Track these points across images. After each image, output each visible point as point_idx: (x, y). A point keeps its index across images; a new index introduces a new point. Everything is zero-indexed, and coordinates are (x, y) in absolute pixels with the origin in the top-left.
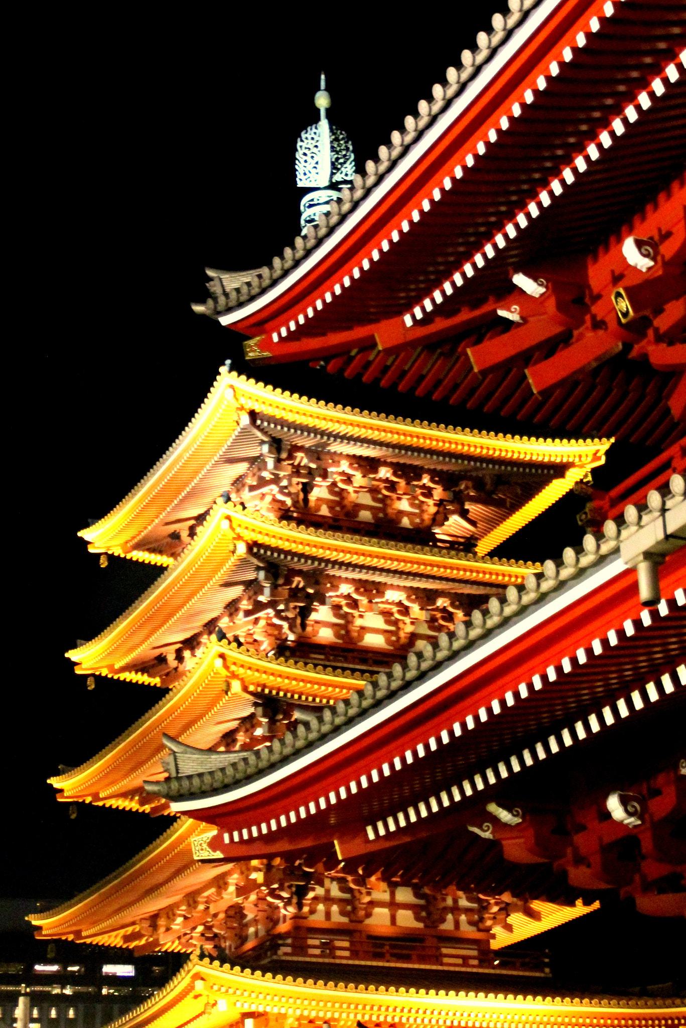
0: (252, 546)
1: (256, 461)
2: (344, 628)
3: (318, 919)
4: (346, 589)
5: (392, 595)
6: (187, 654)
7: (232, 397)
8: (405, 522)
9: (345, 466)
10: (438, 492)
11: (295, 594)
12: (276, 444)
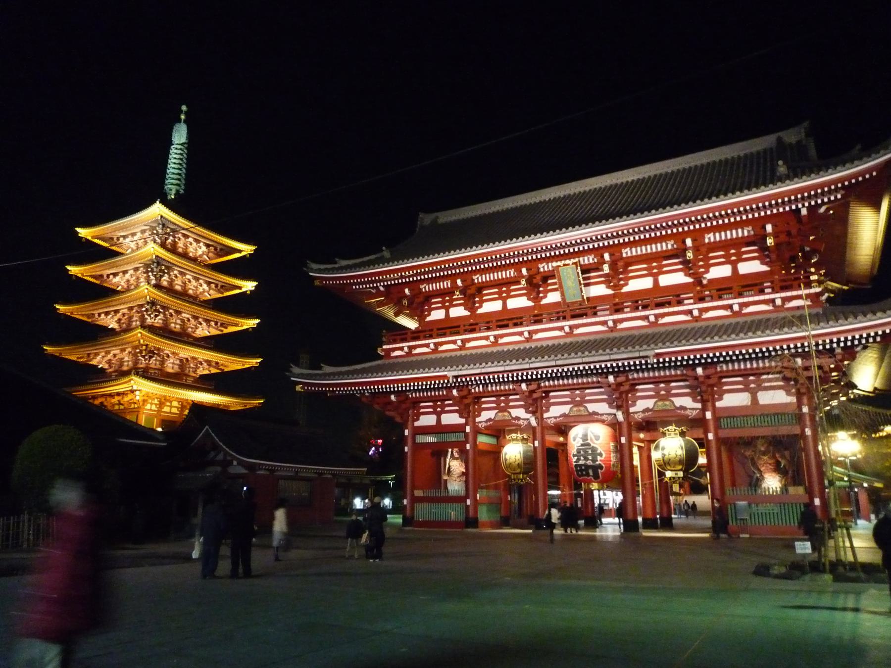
0: (157, 256)
1: (153, 228)
2: (171, 282)
3: (153, 366)
4: (176, 272)
5: (188, 277)
6: (111, 277)
7: (158, 210)
8: (191, 255)
9: (180, 235)
10: (204, 248)
11: (161, 271)
12: (163, 225)
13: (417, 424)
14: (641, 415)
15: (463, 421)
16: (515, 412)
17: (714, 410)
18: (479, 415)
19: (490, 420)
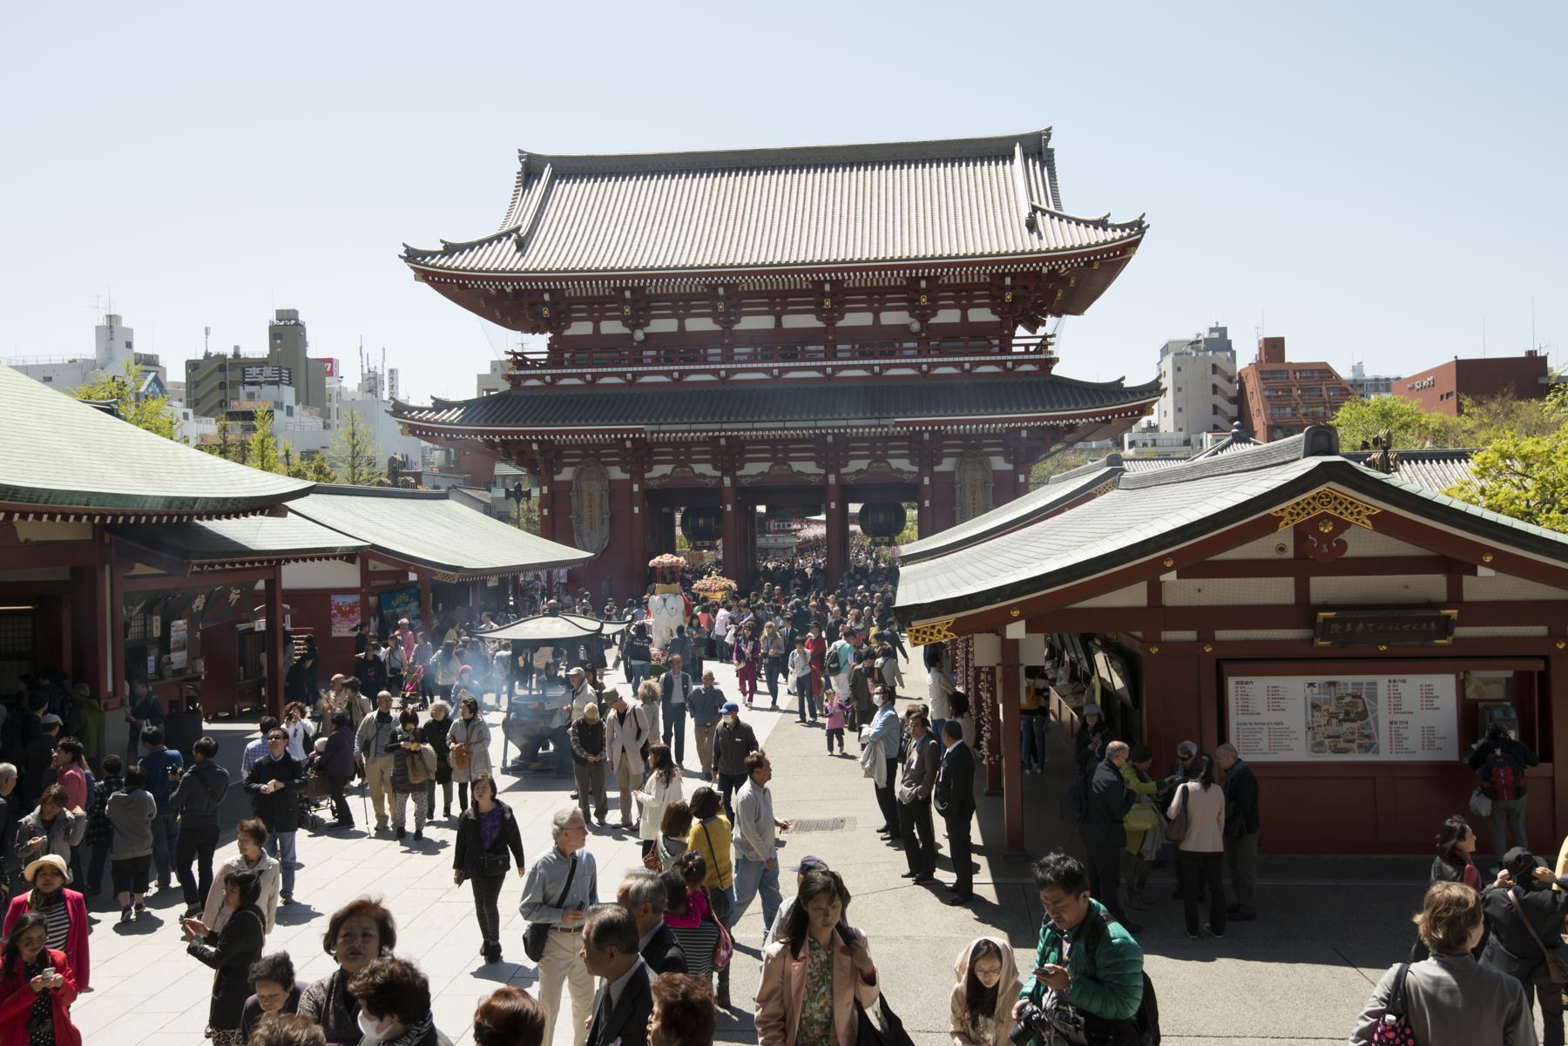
13: (557, 478)
14: (854, 477)
15: (627, 476)
16: (700, 468)
17: (932, 475)
18: (650, 470)
19: (664, 476)
